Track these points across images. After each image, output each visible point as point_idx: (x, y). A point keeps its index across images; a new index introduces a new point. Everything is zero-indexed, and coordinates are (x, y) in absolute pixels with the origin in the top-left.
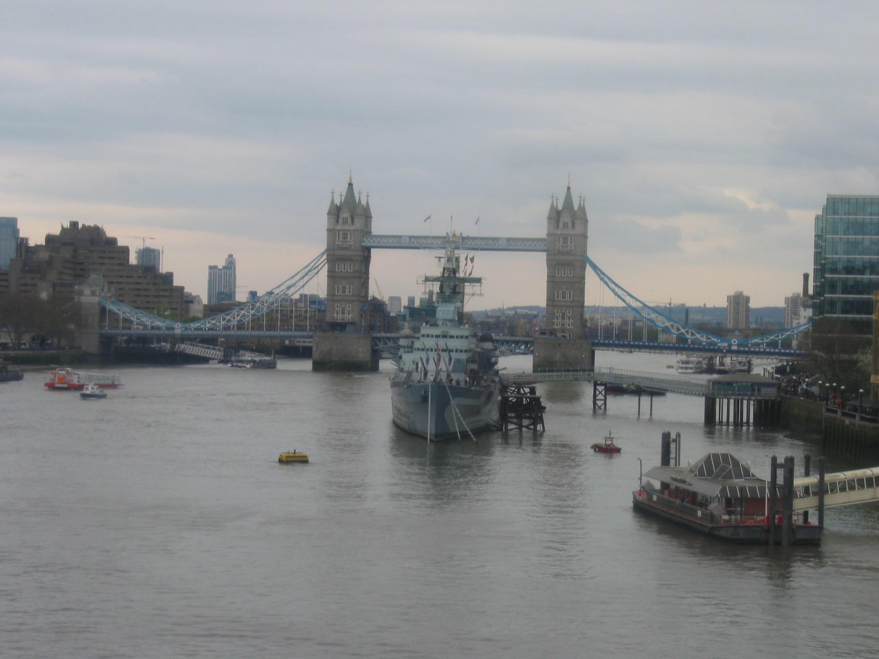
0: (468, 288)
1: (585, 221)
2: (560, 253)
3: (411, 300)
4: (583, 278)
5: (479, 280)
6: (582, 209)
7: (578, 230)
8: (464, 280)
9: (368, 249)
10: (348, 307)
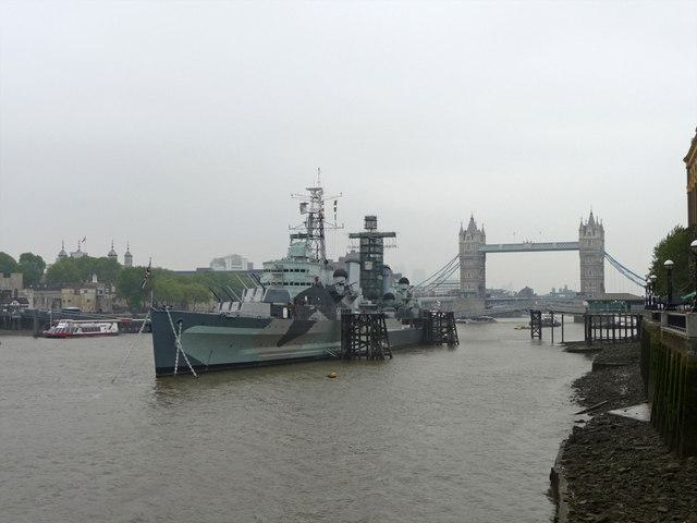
0: (386, 241)
1: (602, 232)
2: (587, 250)
3: (554, 290)
4: (602, 263)
5: (393, 235)
6: (601, 226)
7: (597, 235)
8: (382, 236)
9: (484, 253)
10: (472, 284)
